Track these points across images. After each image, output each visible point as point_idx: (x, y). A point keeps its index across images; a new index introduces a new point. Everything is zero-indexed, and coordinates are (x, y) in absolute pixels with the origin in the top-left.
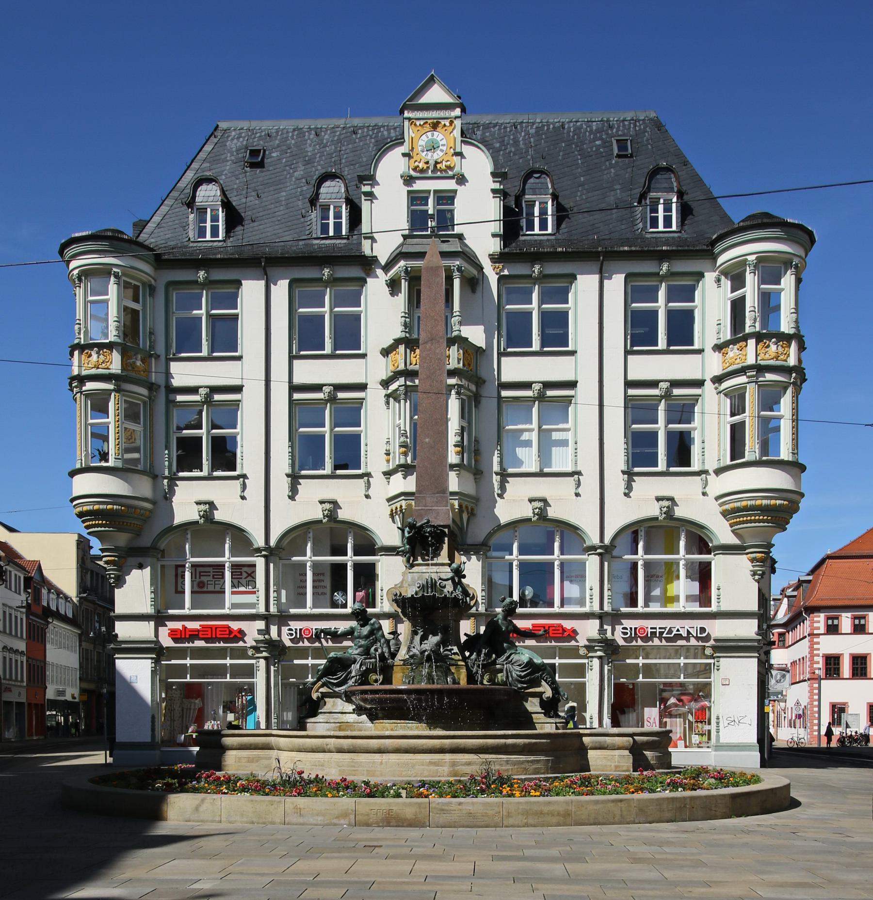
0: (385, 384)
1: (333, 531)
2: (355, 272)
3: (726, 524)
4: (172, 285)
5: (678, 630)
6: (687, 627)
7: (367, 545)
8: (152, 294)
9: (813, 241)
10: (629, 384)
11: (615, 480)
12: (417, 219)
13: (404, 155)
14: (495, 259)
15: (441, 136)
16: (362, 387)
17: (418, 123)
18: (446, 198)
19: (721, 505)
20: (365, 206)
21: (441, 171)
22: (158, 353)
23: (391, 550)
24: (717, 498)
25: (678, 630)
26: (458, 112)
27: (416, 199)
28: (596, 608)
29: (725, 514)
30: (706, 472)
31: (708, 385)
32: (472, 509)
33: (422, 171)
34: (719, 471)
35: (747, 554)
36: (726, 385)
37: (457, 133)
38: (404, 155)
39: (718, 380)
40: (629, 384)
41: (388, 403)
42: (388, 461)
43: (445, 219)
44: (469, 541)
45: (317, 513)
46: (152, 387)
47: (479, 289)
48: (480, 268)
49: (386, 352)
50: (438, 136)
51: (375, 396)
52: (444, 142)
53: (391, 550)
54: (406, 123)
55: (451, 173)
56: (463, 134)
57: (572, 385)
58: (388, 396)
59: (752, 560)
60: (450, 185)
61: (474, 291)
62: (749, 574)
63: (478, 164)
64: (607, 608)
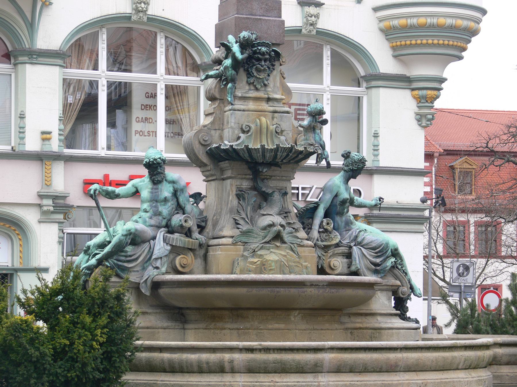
19: (381, 20)
24: (376, 9)
29: (389, 33)
35: (413, 90)
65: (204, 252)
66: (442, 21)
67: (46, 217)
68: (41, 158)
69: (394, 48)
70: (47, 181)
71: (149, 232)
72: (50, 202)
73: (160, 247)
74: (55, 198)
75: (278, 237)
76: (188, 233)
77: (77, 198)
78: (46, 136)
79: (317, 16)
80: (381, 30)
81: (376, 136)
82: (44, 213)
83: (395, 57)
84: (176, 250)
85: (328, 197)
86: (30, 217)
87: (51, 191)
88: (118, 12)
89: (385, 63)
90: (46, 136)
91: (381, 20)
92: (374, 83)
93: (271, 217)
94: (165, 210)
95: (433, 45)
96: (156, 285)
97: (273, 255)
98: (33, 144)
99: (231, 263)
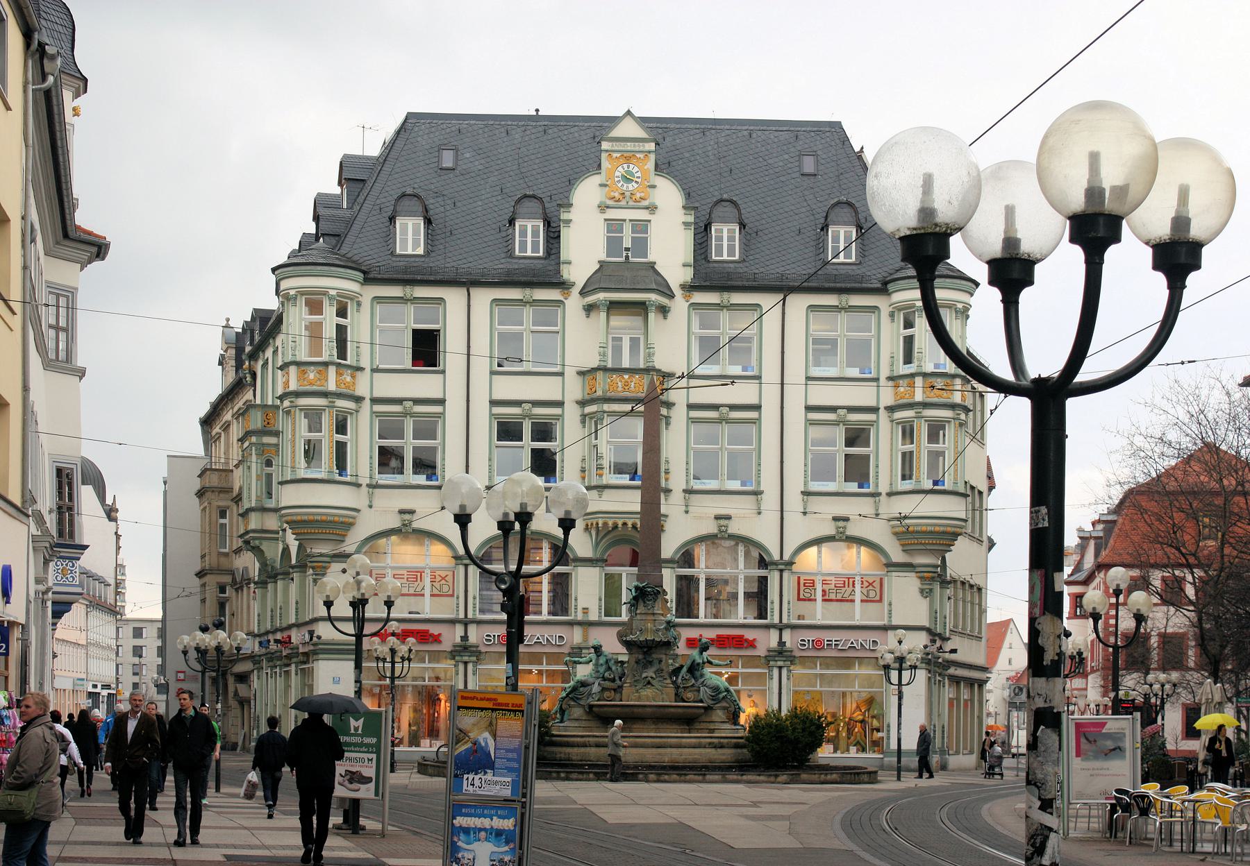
0: (582, 403)
2: (553, 294)
3: (897, 543)
4: (378, 299)
8: (358, 311)
11: (794, 501)
12: (613, 244)
13: (601, 185)
14: (689, 288)
15: (636, 169)
16: (560, 404)
17: (615, 155)
18: (641, 227)
19: (893, 527)
20: (564, 232)
21: (636, 201)
22: (362, 365)
26: (652, 146)
27: (614, 226)
28: (776, 620)
30: (879, 494)
31: (882, 411)
33: (619, 201)
34: (890, 494)
37: (651, 165)
38: (601, 185)
39: (891, 409)
40: (809, 409)
41: (583, 422)
42: (584, 478)
43: (641, 245)
46: (358, 399)
47: (670, 315)
48: (671, 296)
49: (581, 373)
51: (571, 414)
52: (639, 174)
54: (604, 155)
56: (657, 166)
58: (584, 416)
59: (920, 578)
61: (665, 318)
62: (917, 590)
63: (668, 195)
64: (785, 621)
65: (618, 690)
69: (903, 545)
71: (591, 680)
73: (596, 688)
75: (649, 683)
76: (613, 680)
79: (845, 528)
80: (896, 534)
81: (890, 604)
84: (604, 689)
85: (689, 663)
89: (897, 555)
93: (650, 673)
94: (602, 669)
96: (591, 707)
97: (648, 692)
99: (632, 696)
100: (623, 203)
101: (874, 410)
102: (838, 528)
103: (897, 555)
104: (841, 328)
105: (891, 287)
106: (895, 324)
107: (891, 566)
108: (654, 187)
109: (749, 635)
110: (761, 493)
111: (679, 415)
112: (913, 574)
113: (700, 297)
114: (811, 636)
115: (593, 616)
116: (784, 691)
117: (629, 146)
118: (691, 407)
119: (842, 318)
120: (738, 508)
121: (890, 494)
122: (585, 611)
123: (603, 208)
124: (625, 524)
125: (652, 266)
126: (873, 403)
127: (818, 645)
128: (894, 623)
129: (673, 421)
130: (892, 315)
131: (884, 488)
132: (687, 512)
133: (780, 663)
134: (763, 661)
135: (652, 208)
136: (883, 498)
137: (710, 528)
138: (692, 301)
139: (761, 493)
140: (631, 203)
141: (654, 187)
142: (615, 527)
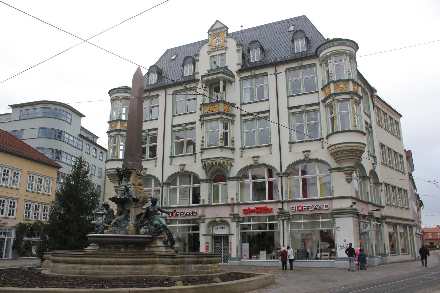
1: (185, 175)
5: (316, 207)
6: (319, 205)
7: (197, 180)
9: (358, 48)
10: (289, 108)
11: (285, 146)
13: (208, 46)
14: (240, 72)
21: (220, 48)
23: (204, 181)
25: (316, 207)
29: (333, 154)
30: (323, 139)
31: (321, 104)
32: (231, 163)
33: (214, 49)
36: (327, 102)
39: (324, 101)
40: (289, 108)
44: (231, 175)
45: (178, 170)
48: (233, 76)
50: (219, 38)
53: (204, 181)
55: (223, 48)
57: (268, 111)
59: (346, 174)
60: (223, 52)
64: (284, 199)
66: (354, 148)
67: (233, 220)
68: (232, 205)
69: (335, 159)
70: (232, 210)
72: (233, 216)
74: (234, 215)
77: (242, 215)
78: (232, 199)
82: (232, 219)
83: (336, 162)
86: (229, 221)
87: (233, 213)
88: (263, 163)
89: (334, 165)
90: (232, 199)
91: (330, 151)
92: (332, 171)
95: (345, 156)
98: (229, 202)
100: (216, 49)
101: (318, 104)
102: (305, 155)
103: (334, 165)
104: (302, 75)
105: (318, 53)
106: (322, 68)
107: (332, 170)
108: (226, 41)
109: (269, 206)
110: (271, 145)
111: (238, 119)
112: (342, 172)
113: (244, 75)
114: (296, 205)
115: (207, 203)
116: (285, 231)
117: (218, 31)
118: (242, 116)
119: (301, 71)
120: (262, 153)
121: (327, 137)
122: (204, 201)
123: (209, 52)
124: (216, 163)
125: (226, 68)
126: (316, 101)
127: (300, 209)
128: (335, 195)
129: (235, 122)
130: (321, 65)
131: (324, 136)
132: (241, 157)
133: (283, 218)
134: (330, 215)
135: (226, 49)
136: (325, 140)
137: (251, 162)
138: (241, 76)
139: (271, 145)
140: (219, 49)
141: (226, 41)
142: (212, 165)
